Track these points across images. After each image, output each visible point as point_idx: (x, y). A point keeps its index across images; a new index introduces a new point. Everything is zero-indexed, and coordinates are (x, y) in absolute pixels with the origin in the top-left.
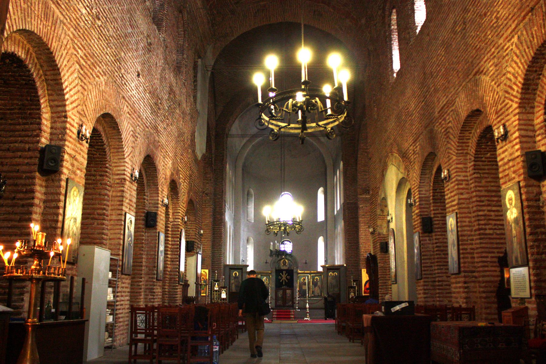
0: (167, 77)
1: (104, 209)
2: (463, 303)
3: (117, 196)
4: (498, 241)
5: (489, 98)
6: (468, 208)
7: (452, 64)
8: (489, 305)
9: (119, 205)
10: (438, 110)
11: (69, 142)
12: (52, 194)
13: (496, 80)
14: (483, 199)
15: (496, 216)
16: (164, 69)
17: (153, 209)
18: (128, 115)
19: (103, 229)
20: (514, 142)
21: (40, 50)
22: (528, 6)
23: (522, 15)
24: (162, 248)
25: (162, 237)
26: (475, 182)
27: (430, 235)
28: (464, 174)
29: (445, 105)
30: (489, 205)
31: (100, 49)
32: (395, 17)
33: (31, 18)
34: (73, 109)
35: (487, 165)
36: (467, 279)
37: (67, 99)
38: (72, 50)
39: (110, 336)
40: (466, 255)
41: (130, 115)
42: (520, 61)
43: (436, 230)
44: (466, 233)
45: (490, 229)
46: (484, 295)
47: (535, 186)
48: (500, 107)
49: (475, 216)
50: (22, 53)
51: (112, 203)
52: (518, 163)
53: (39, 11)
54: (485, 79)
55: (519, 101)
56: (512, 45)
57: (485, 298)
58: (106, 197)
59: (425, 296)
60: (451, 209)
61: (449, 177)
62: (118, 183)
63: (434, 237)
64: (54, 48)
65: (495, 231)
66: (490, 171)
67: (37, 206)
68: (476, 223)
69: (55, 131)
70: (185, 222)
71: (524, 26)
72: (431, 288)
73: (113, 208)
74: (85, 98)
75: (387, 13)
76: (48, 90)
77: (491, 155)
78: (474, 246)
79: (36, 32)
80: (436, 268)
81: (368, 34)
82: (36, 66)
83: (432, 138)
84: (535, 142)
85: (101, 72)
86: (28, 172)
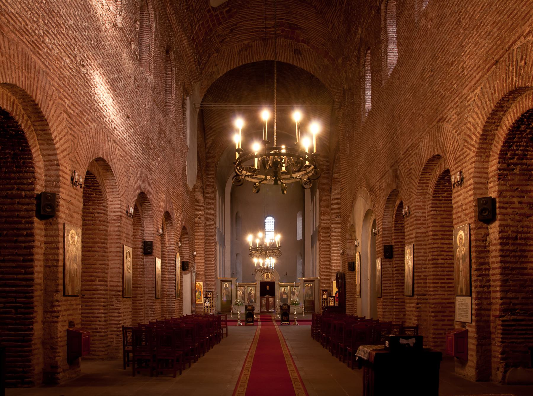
0: (156, 118)
2: (415, 320)
3: (115, 231)
4: (448, 269)
5: (449, 146)
6: (424, 241)
7: (418, 109)
8: (437, 322)
9: (117, 239)
10: (403, 152)
11: (64, 188)
12: (51, 236)
13: (457, 129)
14: (437, 233)
15: (448, 248)
16: (152, 111)
17: (149, 238)
18: (120, 157)
20: (469, 188)
21: (25, 102)
22: (493, 58)
23: (487, 67)
26: (432, 218)
27: (391, 260)
28: (422, 211)
29: (409, 147)
30: (442, 239)
31: (87, 97)
32: (369, 58)
33: (12, 71)
34: (65, 157)
35: (444, 203)
36: (419, 301)
37: (58, 148)
38: (58, 100)
40: (420, 281)
41: (122, 157)
42: (481, 112)
43: (396, 256)
44: (421, 262)
45: (442, 259)
46: (433, 314)
47: (484, 228)
48: (458, 154)
49: (430, 248)
50: (7, 105)
52: (470, 207)
53: (19, 62)
54: (448, 127)
55: (477, 150)
56: (475, 96)
57: (434, 317)
59: (384, 310)
60: (409, 241)
61: (409, 213)
62: (115, 220)
63: (394, 262)
64: (39, 99)
65: (446, 261)
66: (445, 209)
67: (38, 247)
68: (429, 254)
69: (49, 179)
71: (487, 79)
72: (390, 304)
74: (76, 145)
75: (362, 54)
76: (38, 140)
77: (448, 194)
78: (427, 274)
79: (18, 85)
80: (395, 288)
81: (344, 74)
82: (23, 116)
83: (396, 176)
84: (487, 189)
85: (90, 119)
86: (27, 218)
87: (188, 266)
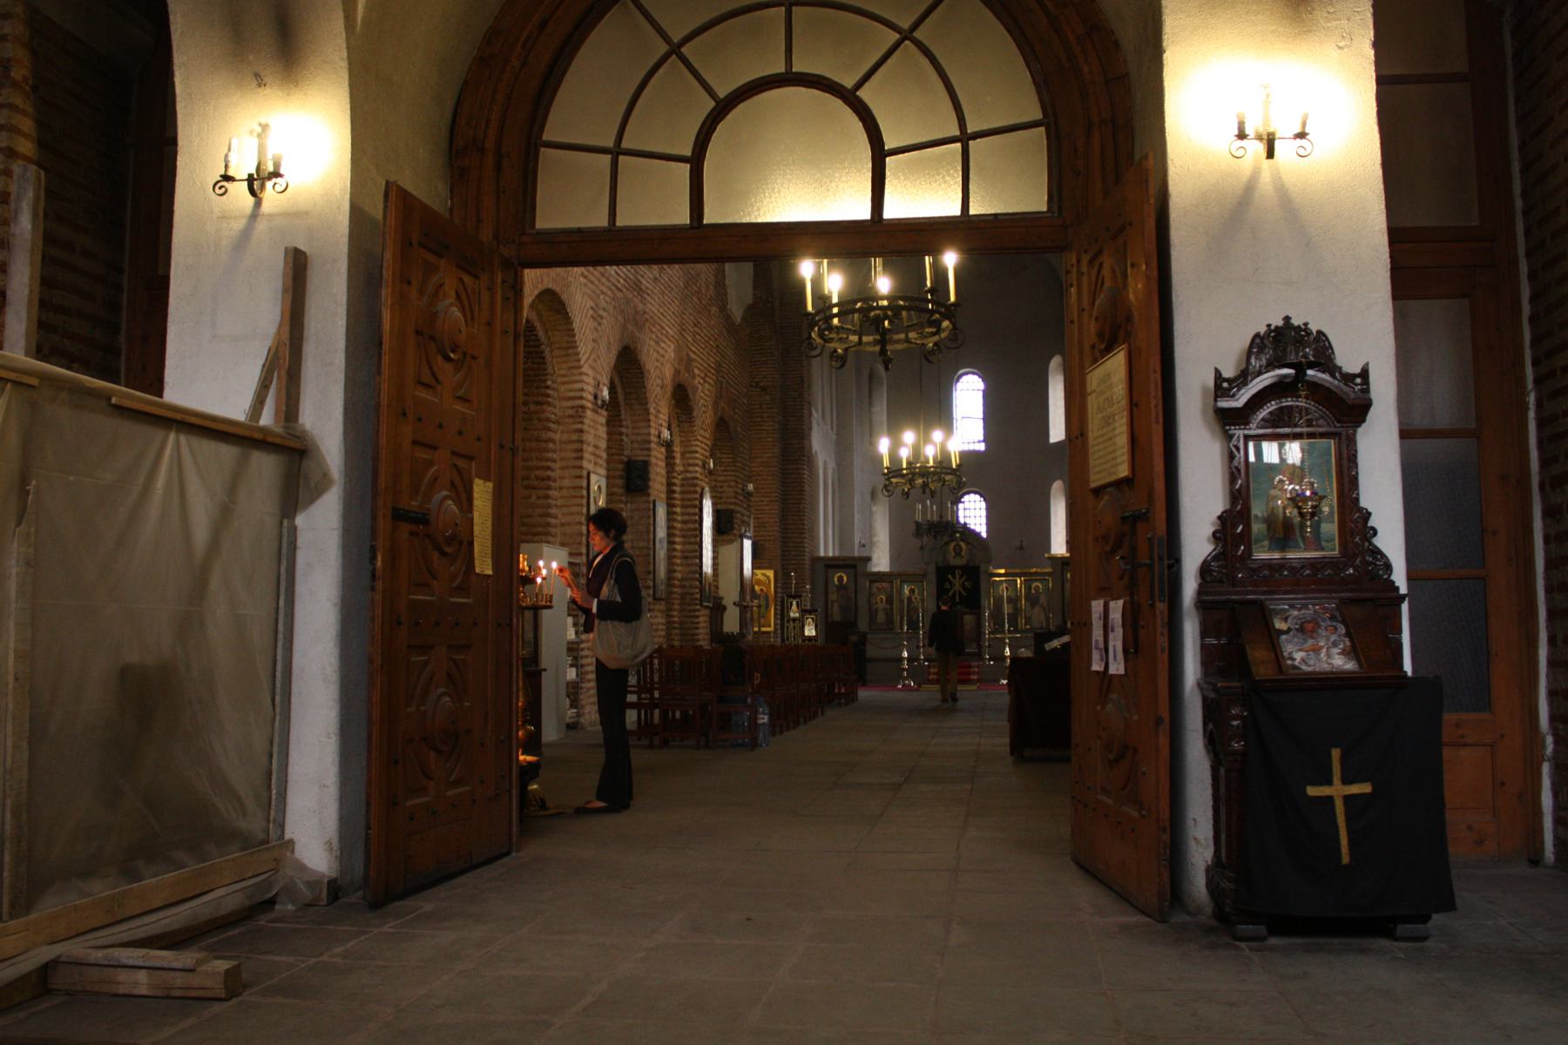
1: (549, 468)
19: (549, 506)
24: (661, 533)
25: (661, 512)
39: (572, 706)
51: (563, 454)
58: (551, 445)
70: (711, 472)
73: (565, 464)
87: (731, 522)
